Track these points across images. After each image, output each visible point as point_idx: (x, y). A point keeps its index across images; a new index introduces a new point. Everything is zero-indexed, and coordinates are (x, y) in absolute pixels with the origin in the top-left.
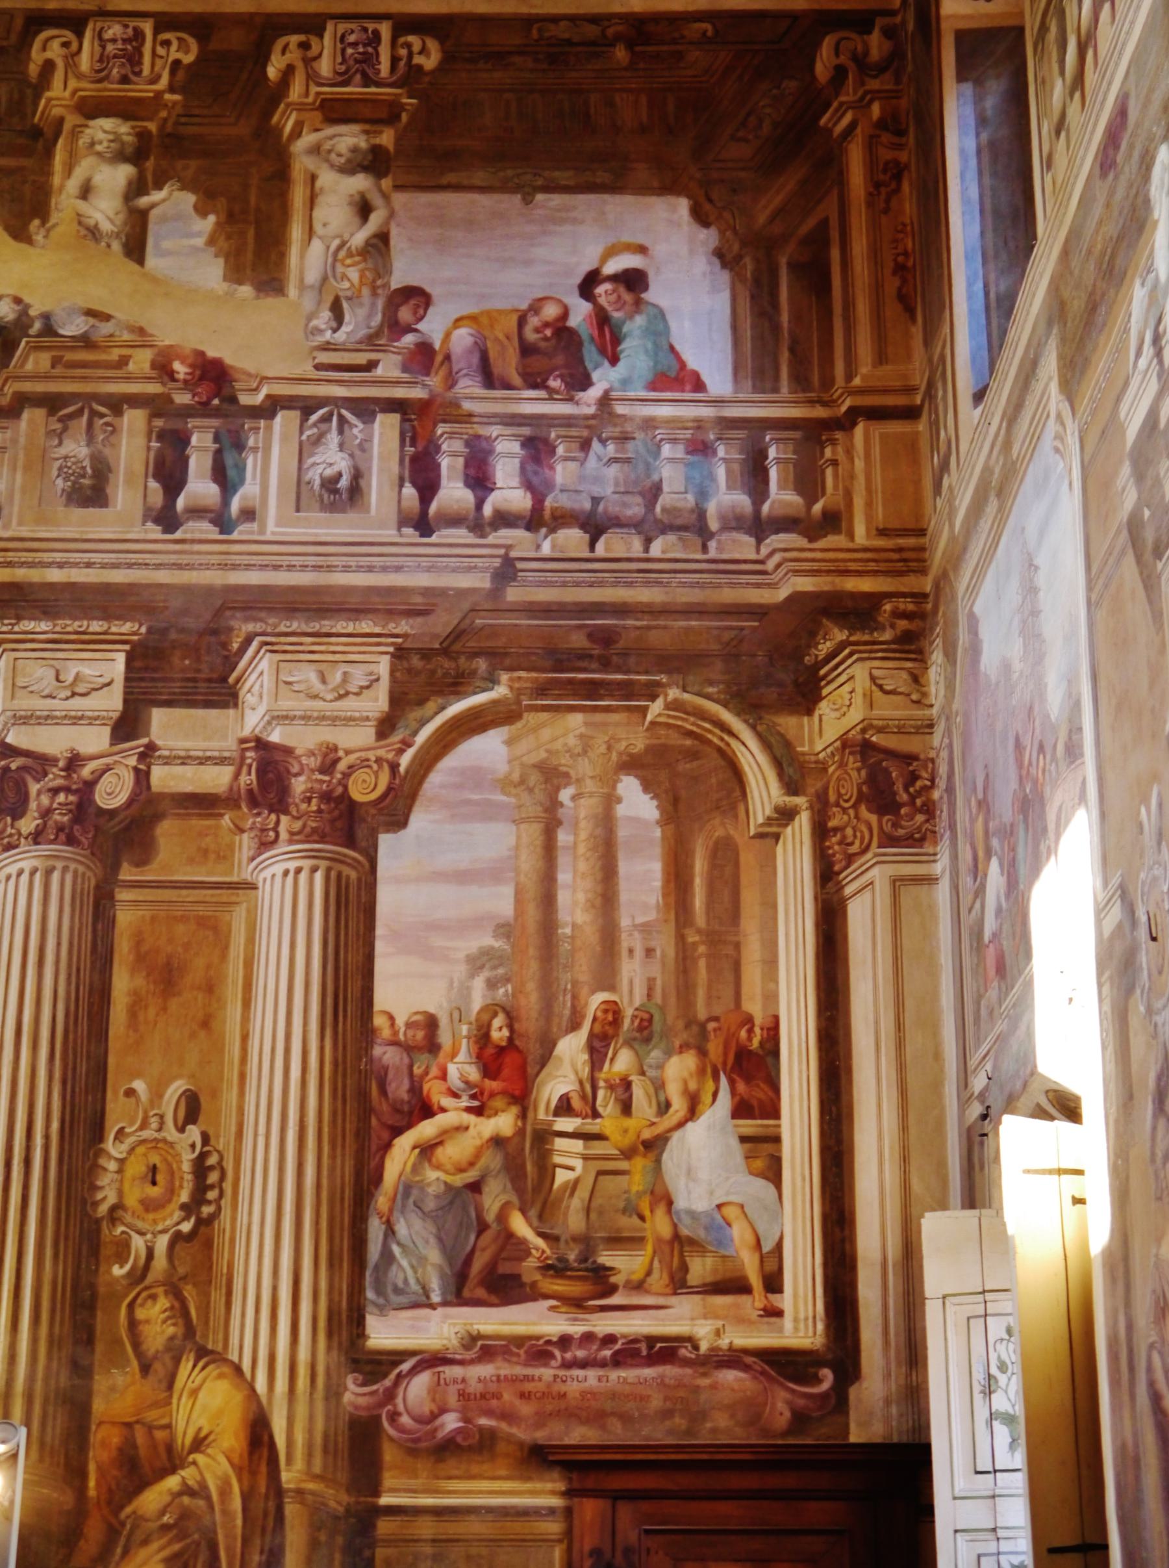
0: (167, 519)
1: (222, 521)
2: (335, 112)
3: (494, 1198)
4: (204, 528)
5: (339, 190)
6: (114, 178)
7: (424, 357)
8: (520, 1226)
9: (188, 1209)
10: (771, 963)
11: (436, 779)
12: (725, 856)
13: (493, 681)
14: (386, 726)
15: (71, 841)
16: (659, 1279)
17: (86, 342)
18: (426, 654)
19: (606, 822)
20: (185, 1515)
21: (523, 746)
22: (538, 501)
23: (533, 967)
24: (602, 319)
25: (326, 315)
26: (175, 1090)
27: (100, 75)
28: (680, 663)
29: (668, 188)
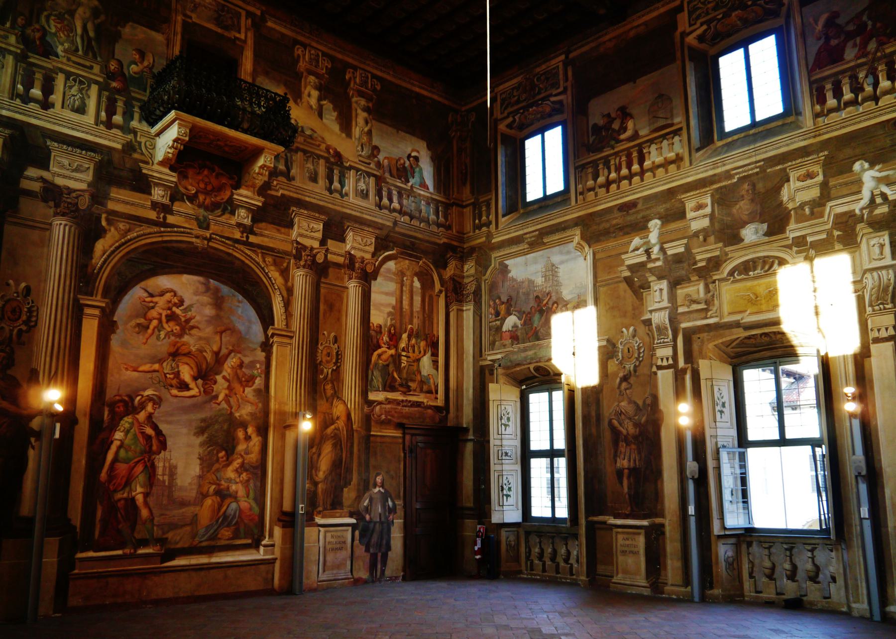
0: (331, 191)
1: (342, 196)
2: (361, 94)
3: (391, 368)
4: (337, 195)
5: (362, 115)
6: (315, 94)
7: (379, 165)
8: (396, 375)
9: (335, 364)
10: (438, 323)
11: (382, 270)
12: (431, 297)
13: (393, 250)
14: (374, 255)
15: (311, 269)
16: (418, 389)
17: (311, 137)
18: (382, 239)
19: (412, 286)
20: (336, 435)
21: (398, 265)
22: (401, 208)
23: (398, 317)
24: (411, 167)
25: (359, 148)
26: (333, 334)
27: (310, 62)
28: (425, 253)
29: (422, 139)
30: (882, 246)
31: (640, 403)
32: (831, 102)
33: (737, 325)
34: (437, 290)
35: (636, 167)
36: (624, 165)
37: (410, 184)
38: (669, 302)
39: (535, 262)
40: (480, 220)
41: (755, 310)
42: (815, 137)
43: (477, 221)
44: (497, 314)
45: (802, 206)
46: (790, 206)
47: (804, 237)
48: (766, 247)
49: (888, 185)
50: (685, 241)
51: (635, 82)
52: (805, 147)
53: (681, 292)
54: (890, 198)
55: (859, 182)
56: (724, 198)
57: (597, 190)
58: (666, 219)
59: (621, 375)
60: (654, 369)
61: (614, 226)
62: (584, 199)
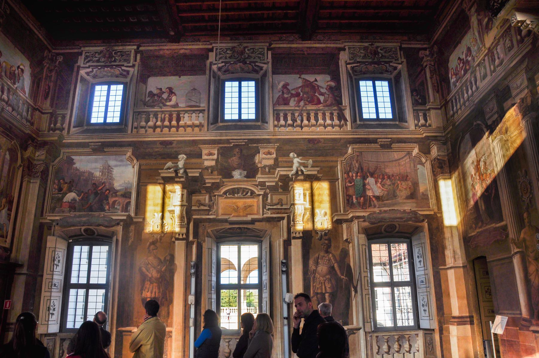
30: (300, 194)
31: (162, 259)
32: (282, 122)
33: (226, 221)
34: (18, 165)
35: (174, 123)
36: (167, 119)
37: (16, 86)
38: (187, 202)
39: (96, 161)
40: (55, 125)
41: (236, 215)
42: (274, 135)
43: (52, 125)
44: (60, 189)
45: (265, 167)
46: (259, 165)
47: (265, 182)
48: (245, 183)
49: (304, 167)
50: (200, 171)
51: (180, 77)
52: (268, 139)
53: (195, 198)
54: (305, 173)
55: (292, 162)
56: (225, 152)
57: (147, 128)
58: (190, 156)
59: (151, 240)
60: (173, 239)
61: (156, 152)
62: (137, 132)
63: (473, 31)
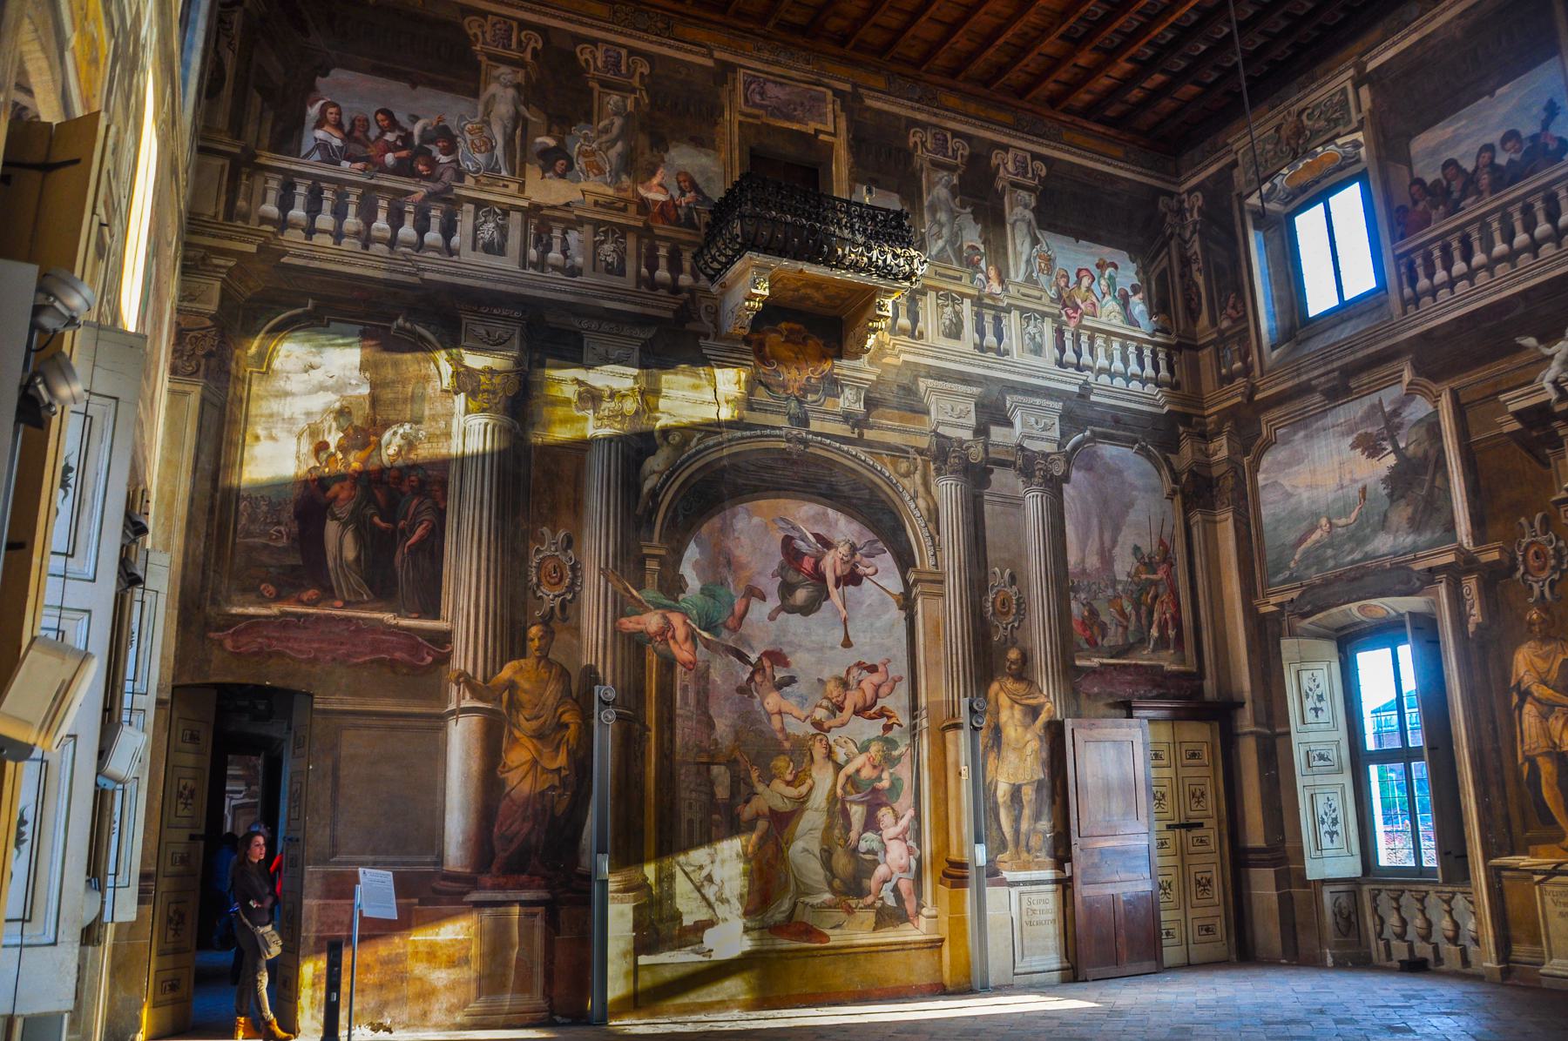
63: (487, 113)
